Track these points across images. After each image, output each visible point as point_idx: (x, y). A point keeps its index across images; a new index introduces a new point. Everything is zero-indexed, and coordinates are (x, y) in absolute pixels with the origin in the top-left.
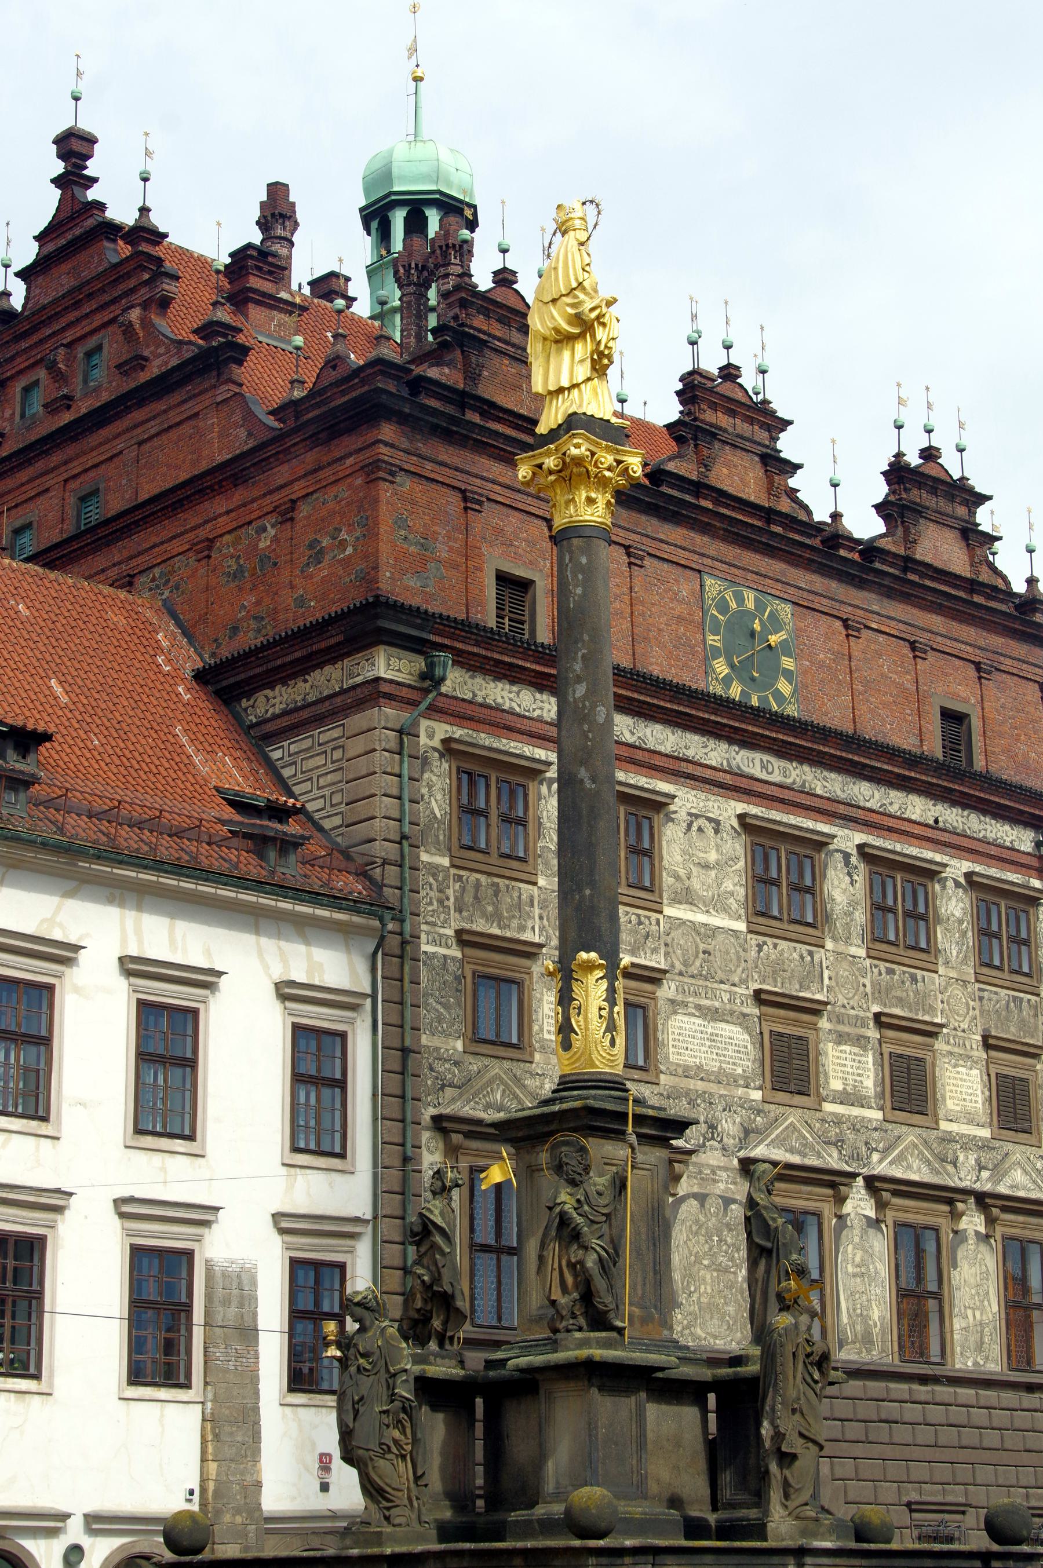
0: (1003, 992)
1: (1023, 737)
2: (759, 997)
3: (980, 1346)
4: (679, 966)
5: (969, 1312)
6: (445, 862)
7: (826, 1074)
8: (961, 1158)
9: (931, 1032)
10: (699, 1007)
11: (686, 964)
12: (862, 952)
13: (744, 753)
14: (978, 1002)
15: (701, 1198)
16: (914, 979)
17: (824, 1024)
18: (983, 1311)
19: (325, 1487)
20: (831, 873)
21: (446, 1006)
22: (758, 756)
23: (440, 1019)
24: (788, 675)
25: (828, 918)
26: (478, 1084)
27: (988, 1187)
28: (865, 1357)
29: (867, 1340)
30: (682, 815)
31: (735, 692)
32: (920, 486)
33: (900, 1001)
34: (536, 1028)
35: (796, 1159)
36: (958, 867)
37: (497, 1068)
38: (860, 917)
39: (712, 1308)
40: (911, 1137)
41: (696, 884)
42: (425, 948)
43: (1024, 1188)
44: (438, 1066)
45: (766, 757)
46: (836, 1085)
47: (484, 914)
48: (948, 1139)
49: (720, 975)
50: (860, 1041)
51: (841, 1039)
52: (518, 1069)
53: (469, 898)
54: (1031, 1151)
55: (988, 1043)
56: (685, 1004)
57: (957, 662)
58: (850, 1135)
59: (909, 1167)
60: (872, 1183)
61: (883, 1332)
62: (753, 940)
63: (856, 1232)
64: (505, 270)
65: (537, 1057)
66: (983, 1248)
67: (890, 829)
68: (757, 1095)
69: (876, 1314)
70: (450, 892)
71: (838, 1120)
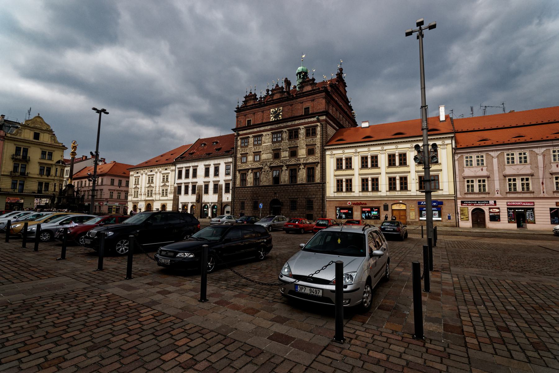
0: (310, 139)
2: (273, 150)
3: (302, 181)
9: (298, 147)
15: (264, 171)
16: (295, 142)
17: (281, 150)
18: (303, 176)
24: (281, 115)
25: (283, 139)
29: (285, 182)
36: (301, 127)
37: (244, 164)
38: (287, 137)
39: (265, 181)
41: (266, 141)
46: (283, 156)
48: (299, 158)
50: (286, 151)
51: (283, 151)
52: (246, 164)
54: (313, 157)
55: (307, 145)
66: (304, 170)
68: (272, 160)
69: (286, 179)
71: (283, 160)
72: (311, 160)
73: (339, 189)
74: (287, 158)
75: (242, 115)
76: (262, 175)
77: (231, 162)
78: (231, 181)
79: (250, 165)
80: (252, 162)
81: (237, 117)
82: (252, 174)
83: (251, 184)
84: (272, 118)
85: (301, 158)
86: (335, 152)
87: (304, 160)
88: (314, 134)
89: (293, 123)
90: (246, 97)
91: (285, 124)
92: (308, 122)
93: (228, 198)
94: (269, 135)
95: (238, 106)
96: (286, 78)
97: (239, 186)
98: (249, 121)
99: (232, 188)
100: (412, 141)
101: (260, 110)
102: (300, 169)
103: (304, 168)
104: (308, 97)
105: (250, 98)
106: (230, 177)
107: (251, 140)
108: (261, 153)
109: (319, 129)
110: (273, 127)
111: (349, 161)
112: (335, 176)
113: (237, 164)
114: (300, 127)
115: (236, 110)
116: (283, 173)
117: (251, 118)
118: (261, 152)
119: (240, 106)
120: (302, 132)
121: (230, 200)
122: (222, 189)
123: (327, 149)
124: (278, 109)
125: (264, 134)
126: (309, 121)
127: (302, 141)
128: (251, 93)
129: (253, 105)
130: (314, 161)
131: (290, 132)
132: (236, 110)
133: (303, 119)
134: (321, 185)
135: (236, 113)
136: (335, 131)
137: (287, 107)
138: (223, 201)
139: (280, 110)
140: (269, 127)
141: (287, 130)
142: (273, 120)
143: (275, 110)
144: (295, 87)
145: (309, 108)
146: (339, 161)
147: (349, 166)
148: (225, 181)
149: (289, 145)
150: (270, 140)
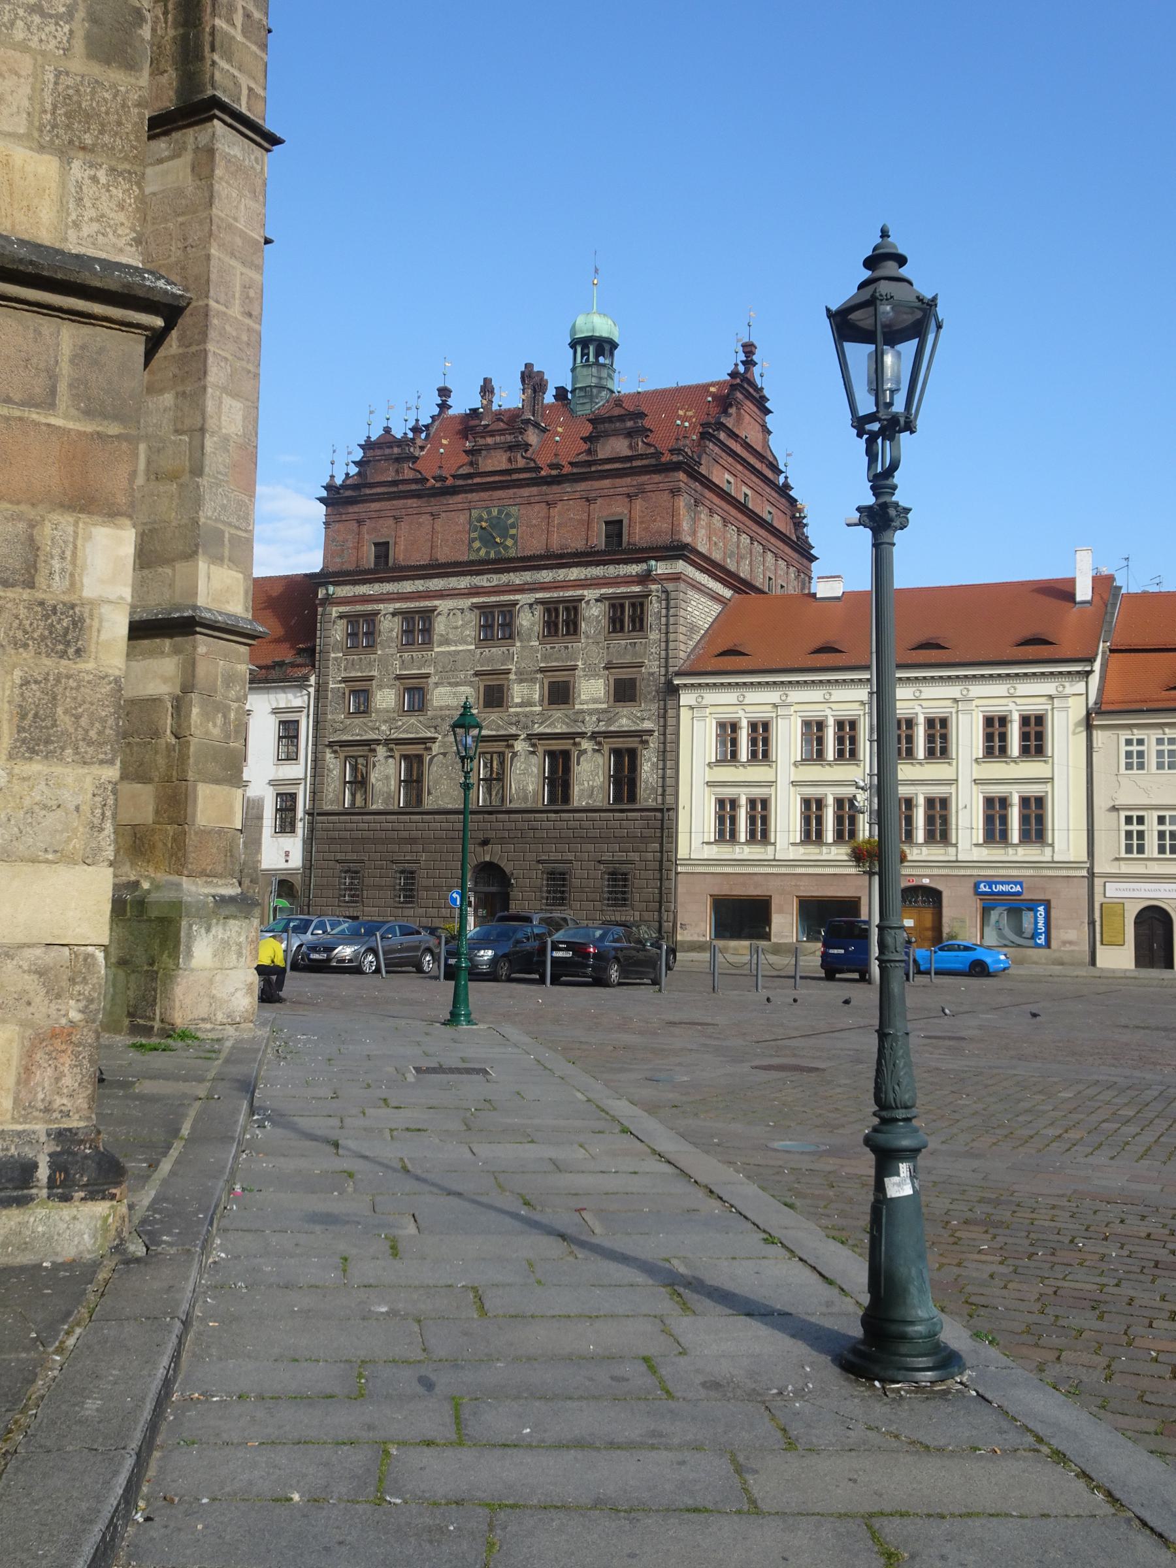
1: (659, 519)
3: (591, 796)
4: (440, 670)
5: (585, 783)
6: (341, 655)
7: (513, 697)
8: (587, 718)
10: (449, 683)
11: (443, 667)
12: (537, 643)
13: (479, 578)
14: (605, 651)
15: (444, 754)
16: (567, 648)
17: (512, 677)
18: (594, 780)
19: (287, 861)
20: (521, 614)
21: (339, 704)
22: (485, 577)
23: (336, 709)
24: (513, 537)
26: (348, 728)
27: (603, 729)
28: (523, 806)
29: (525, 799)
30: (446, 611)
31: (483, 552)
32: (603, 423)
33: (556, 660)
34: (373, 705)
35: (494, 733)
37: (356, 721)
40: (558, 714)
41: (451, 636)
42: (331, 686)
43: (627, 726)
44: (335, 725)
45: (489, 576)
46: (517, 700)
47: (357, 671)
48: (582, 712)
49: (461, 668)
50: (533, 681)
51: (521, 681)
52: (365, 720)
53: (350, 665)
56: (442, 683)
57: (618, 497)
58: (523, 719)
59: (555, 727)
60: (529, 737)
61: (534, 795)
62: (479, 651)
63: (523, 757)
64: (388, 427)
65: (373, 715)
66: (597, 755)
67: (555, 588)
69: (531, 788)
70: (343, 665)
71: (517, 714)
72: (624, 722)
73: (726, 832)
74: (534, 709)
75: (351, 517)
76: (434, 768)
77: (299, 710)
78: (302, 787)
79: (383, 728)
80: (392, 715)
81: (327, 524)
82: (391, 760)
83: (385, 802)
84: (477, 544)
85: (591, 713)
86: (710, 697)
87: (599, 721)
88: (639, 624)
89: (561, 574)
90: (368, 446)
91: (527, 577)
92: (618, 576)
93: (287, 854)
94: (462, 611)
95: (332, 477)
96: (528, 366)
97: (334, 808)
98: (382, 549)
99: (306, 813)
100: (966, 676)
101: (429, 509)
102: (585, 751)
103: (598, 751)
104: (618, 482)
105: (387, 451)
106: (295, 771)
107: (390, 627)
108: (433, 680)
109: (654, 606)
110: (482, 581)
111: (761, 732)
112: (709, 784)
113: (329, 717)
114: (585, 592)
115: (324, 494)
116: (519, 765)
117: (385, 530)
118: (427, 676)
119: (339, 481)
120: (594, 613)
121: (296, 861)
122: (260, 818)
123: (685, 685)
124: (500, 512)
125: (443, 605)
126: (621, 573)
127: (594, 648)
128: (387, 430)
129: (394, 483)
130: (639, 728)
131: (551, 608)
132: (324, 494)
133: (598, 564)
134: (659, 815)
135: (324, 507)
136: (718, 608)
137: (537, 507)
138: (265, 865)
139: (508, 515)
140: (463, 582)
141: (539, 602)
142: (483, 552)
143: (489, 513)
144: (561, 393)
145: (621, 522)
146: (727, 731)
147: (762, 749)
148: (273, 783)
149: (545, 658)
150: (470, 632)
